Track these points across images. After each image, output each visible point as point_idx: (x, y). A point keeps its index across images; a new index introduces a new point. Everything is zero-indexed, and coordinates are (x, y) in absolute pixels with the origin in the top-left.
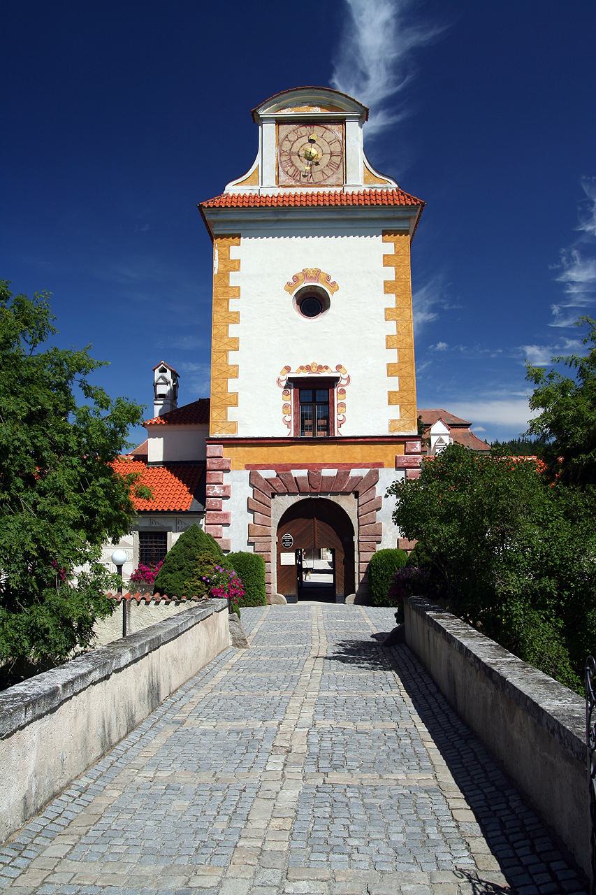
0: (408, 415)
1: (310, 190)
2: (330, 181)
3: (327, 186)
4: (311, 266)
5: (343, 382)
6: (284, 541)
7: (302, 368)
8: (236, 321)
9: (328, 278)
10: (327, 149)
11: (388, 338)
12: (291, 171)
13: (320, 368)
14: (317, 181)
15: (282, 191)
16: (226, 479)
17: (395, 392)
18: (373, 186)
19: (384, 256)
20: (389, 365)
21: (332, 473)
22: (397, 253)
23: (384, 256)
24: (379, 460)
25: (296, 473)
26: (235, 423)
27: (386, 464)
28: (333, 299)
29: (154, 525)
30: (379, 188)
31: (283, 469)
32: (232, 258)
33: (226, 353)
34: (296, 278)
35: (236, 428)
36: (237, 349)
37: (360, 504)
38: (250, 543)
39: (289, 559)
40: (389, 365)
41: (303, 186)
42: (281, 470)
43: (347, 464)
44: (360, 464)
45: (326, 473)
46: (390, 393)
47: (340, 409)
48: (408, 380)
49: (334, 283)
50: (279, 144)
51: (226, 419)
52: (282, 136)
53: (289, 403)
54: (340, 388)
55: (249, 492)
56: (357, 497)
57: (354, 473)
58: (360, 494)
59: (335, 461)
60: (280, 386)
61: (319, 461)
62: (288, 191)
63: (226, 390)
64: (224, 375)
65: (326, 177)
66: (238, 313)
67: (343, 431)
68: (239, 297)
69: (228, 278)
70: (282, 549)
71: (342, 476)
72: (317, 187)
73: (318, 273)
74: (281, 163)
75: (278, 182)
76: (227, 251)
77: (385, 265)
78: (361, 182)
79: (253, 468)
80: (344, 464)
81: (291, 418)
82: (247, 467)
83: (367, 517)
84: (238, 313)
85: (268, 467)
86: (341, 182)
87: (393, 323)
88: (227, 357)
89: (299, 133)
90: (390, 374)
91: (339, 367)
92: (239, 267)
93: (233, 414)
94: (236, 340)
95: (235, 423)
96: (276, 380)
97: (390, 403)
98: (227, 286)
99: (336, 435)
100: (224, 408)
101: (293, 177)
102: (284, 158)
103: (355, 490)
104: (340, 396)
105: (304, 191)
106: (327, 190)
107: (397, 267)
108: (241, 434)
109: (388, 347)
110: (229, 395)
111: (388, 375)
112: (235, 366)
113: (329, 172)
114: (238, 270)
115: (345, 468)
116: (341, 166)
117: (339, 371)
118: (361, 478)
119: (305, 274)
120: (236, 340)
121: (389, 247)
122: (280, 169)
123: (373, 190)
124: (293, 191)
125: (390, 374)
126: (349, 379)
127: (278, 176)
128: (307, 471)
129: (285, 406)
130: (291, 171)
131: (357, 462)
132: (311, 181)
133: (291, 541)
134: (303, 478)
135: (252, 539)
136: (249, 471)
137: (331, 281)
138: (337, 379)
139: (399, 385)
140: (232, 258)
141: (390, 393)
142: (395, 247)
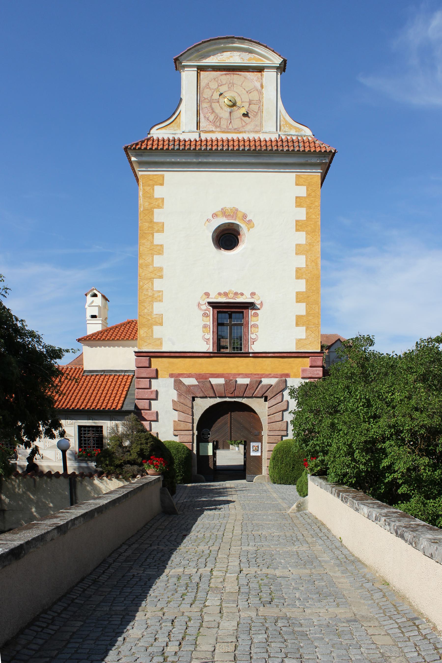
2: (248, 128)
3: (245, 132)
4: (229, 205)
7: (220, 294)
9: (245, 216)
10: (246, 98)
11: (298, 270)
12: (212, 118)
13: (236, 294)
14: (236, 127)
17: (302, 316)
18: (289, 133)
19: (297, 197)
21: (246, 381)
22: (309, 195)
23: (297, 197)
24: (286, 372)
25: (214, 381)
26: (160, 340)
30: (294, 135)
33: (151, 280)
34: (215, 215)
38: (176, 436)
41: (223, 132)
43: (258, 374)
44: (270, 374)
47: (253, 329)
49: (250, 221)
55: (174, 395)
56: (266, 400)
57: (265, 381)
58: (268, 398)
60: (201, 309)
61: (234, 371)
63: (152, 312)
65: (244, 124)
66: (162, 246)
68: (163, 231)
69: (153, 214)
76: (152, 191)
77: (296, 206)
80: (255, 374)
81: (210, 336)
82: (171, 376)
84: (162, 246)
85: (189, 376)
86: (258, 129)
88: (152, 284)
89: (219, 81)
92: (163, 204)
93: (157, 331)
94: (160, 269)
95: (160, 340)
97: (297, 325)
98: (151, 221)
99: (250, 351)
101: (214, 123)
105: (225, 136)
107: (309, 208)
110: (155, 316)
111: (297, 302)
116: (259, 114)
119: (224, 212)
120: (160, 269)
121: (302, 191)
127: (198, 123)
129: (205, 326)
131: (267, 373)
132: (230, 127)
134: (220, 385)
135: (176, 433)
137: (248, 219)
142: (307, 190)
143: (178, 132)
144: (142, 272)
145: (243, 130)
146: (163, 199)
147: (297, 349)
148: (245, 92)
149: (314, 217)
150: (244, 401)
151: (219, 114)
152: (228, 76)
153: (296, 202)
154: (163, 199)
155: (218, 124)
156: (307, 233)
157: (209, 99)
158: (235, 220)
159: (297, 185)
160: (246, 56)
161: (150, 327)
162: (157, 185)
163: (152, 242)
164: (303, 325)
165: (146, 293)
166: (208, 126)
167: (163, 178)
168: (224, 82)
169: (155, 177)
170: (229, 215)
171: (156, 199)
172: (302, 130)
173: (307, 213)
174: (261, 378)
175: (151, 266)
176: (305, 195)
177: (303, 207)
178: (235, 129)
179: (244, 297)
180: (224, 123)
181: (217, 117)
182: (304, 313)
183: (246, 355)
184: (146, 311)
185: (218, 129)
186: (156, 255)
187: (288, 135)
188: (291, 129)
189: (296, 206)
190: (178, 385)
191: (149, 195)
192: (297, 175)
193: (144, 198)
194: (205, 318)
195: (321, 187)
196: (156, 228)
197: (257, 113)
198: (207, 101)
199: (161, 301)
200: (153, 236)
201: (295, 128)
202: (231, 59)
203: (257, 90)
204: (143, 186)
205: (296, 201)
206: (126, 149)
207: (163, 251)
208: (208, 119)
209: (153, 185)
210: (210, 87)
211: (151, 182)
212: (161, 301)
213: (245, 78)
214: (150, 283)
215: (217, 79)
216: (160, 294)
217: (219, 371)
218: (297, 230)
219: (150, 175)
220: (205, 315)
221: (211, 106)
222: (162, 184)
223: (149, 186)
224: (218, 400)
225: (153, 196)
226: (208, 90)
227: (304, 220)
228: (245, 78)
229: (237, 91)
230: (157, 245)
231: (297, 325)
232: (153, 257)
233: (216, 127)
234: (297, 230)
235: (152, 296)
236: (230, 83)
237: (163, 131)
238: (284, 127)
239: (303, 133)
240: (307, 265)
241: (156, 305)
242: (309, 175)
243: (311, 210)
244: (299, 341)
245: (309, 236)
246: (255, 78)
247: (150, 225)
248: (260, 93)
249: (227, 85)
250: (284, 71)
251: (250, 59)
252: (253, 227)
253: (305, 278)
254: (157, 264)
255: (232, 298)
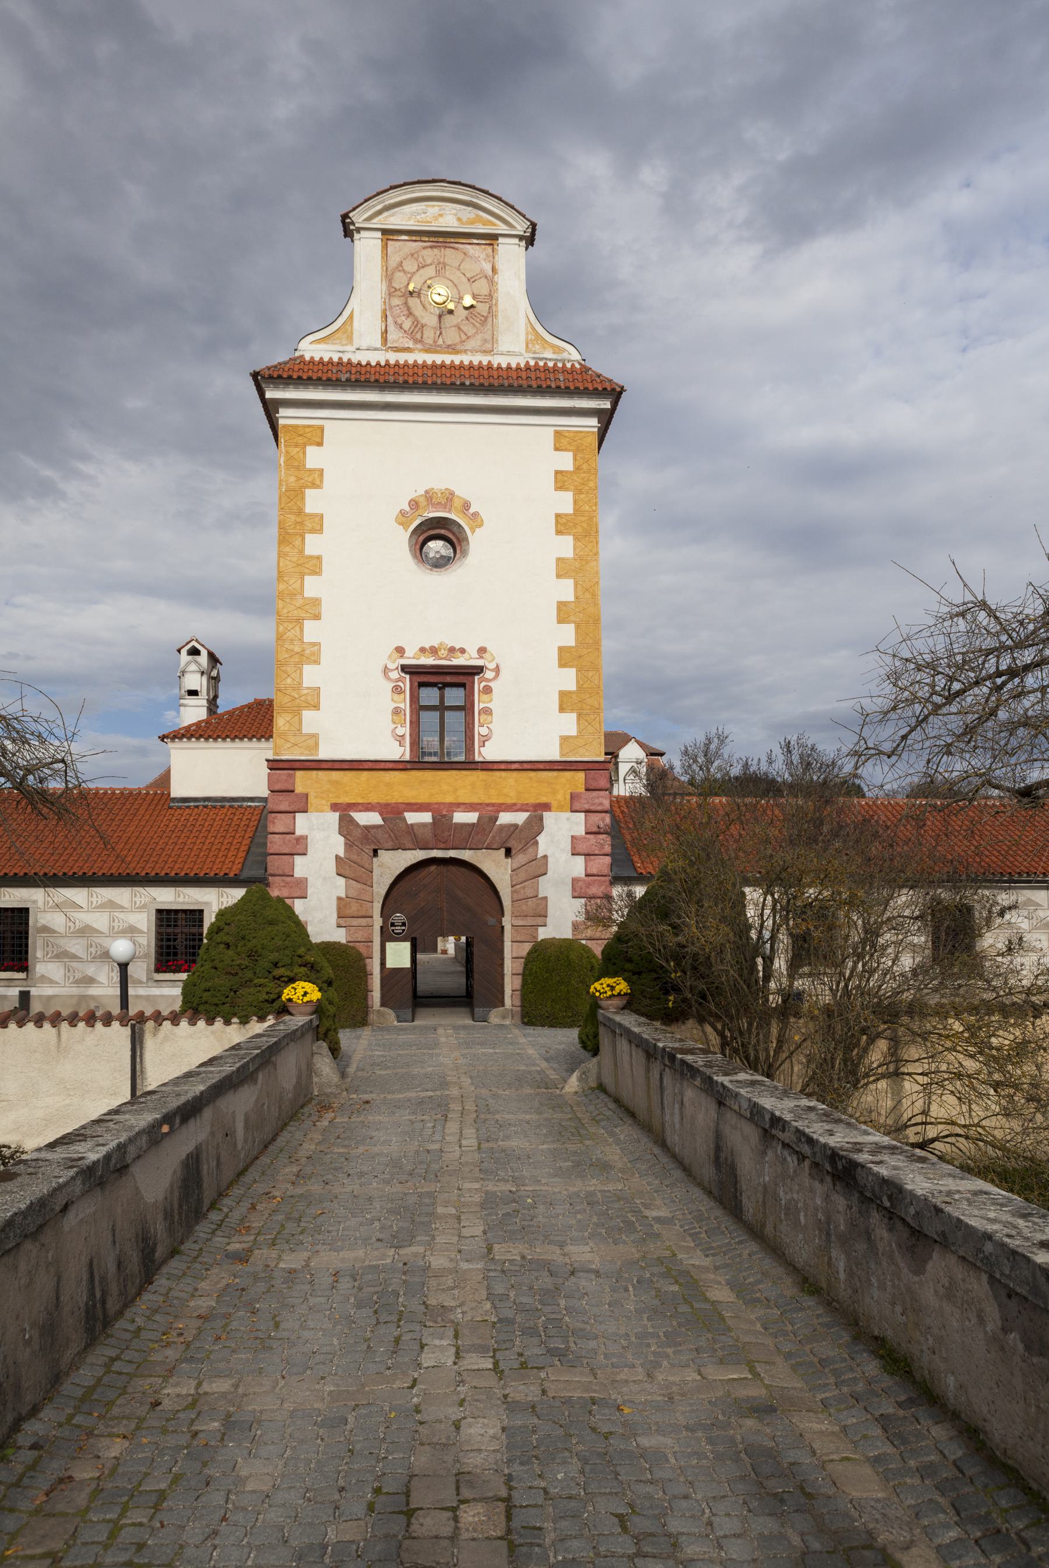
0: (590, 729)
1: (438, 359)
2: (471, 344)
3: (465, 351)
5: (489, 675)
6: (393, 925)
7: (423, 650)
8: (317, 571)
9: (466, 505)
11: (561, 605)
12: (407, 324)
13: (452, 650)
14: (449, 342)
15: (393, 358)
16: (302, 824)
17: (570, 692)
18: (541, 356)
19: (557, 472)
20: (561, 649)
21: (472, 817)
22: (578, 468)
23: (557, 472)
24: (544, 800)
25: (413, 818)
26: (315, 737)
27: (554, 804)
28: (476, 540)
29: (181, 899)
30: (550, 360)
31: (393, 812)
32: (309, 465)
34: (414, 504)
35: (317, 744)
36: (317, 617)
37: (515, 866)
39: (399, 955)
40: (561, 649)
42: (388, 813)
43: (493, 805)
44: (515, 804)
45: (461, 817)
46: (563, 694)
47: (483, 717)
48: (590, 674)
49: (476, 515)
50: (388, 276)
51: (300, 730)
52: (394, 261)
53: (402, 706)
54: (483, 684)
55: (338, 845)
56: (508, 853)
57: (505, 818)
58: (513, 852)
59: (475, 800)
60: (389, 679)
61: (449, 799)
62: (402, 358)
63: (300, 683)
64: (296, 659)
65: (464, 337)
66: (319, 558)
67: (488, 753)
68: (320, 531)
69: (303, 498)
70: (388, 935)
71: (489, 820)
72: (450, 353)
73: (450, 497)
74: (391, 308)
75: (385, 340)
76: (301, 455)
77: (557, 489)
78: (521, 347)
79: (344, 810)
80: (488, 805)
82: (335, 807)
83: (524, 888)
84: (319, 558)
85: (368, 807)
86: (488, 346)
87: (569, 584)
88: (302, 630)
89: (421, 259)
90: (562, 664)
91: (482, 651)
92: (322, 481)
94: (316, 602)
95: (315, 737)
96: (381, 668)
97: (562, 709)
98: (300, 512)
99: (477, 758)
100: (296, 712)
101: (411, 334)
102: (396, 301)
103: (508, 845)
104: (484, 697)
105: (430, 358)
106: (466, 359)
108: (325, 753)
109: (561, 620)
110: (305, 692)
112: (314, 644)
113: (469, 330)
114: (319, 487)
115: (490, 812)
116: (490, 319)
117: (482, 657)
118: (516, 826)
119: (429, 496)
120: (316, 602)
122: (390, 319)
123: (541, 364)
124: (410, 358)
125: (562, 664)
126: (497, 670)
127: (385, 333)
128: (430, 814)
129: (396, 711)
130: (407, 324)
131: (509, 801)
132: (440, 342)
133: (404, 924)
134: (424, 825)
136: (337, 814)
137: (472, 511)
138: (479, 670)
139: (578, 682)
140: (309, 465)
141: (563, 694)
142: (575, 459)
143: (348, 348)
144: (283, 608)
145: (462, 348)
146: (321, 471)
147: (562, 755)
148: (465, 280)
149: (587, 508)
150: (466, 855)
151: (420, 319)
152: (436, 251)
153: (556, 482)
154: (321, 471)
155: (418, 336)
156: (576, 539)
157: (403, 290)
158: (450, 512)
159: (556, 449)
160: (469, 213)
161: (297, 712)
162: (311, 444)
163: (301, 551)
164: (572, 711)
165: (291, 647)
166: (401, 340)
167: (322, 431)
168: (429, 261)
169: (307, 430)
170: (439, 503)
171: (310, 470)
172: (564, 350)
173: (575, 502)
174: (498, 812)
175: (299, 597)
176: (570, 467)
177: (567, 490)
178: (449, 346)
179: (466, 655)
180: (429, 336)
181: (416, 323)
182: (572, 687)
183: (470, 765)
184: (289, 681)
185: (419, 346)
186: (310, 574)
187: (541, 359)
188: (545, 348)
189: (557, 489)
190: (347, 825)
191: (296, 464)
192: (556, 432)
193: (288, 469)
194: (396, 696)
195: (599, 449)
196: (308, 524)
197: (486, 318)
198: (399, 293)
199: (317, 662)
200: (303, 539)
201: (553, 346)
202: (441, 220)
203: (486, 277)
204: (286, 446)
205: (556, 478)
206: (255, 375)
207: (320, 568)
208: (401, 328)
209: (304, 446)
210: (405, 268)
211: (300, 440)
212: (317, 662)
213: (465, 254)
214: (297, 629)
215: (416, 256)
216: (316, 648)
217: (423, 798)
218: (559, 532)
219: (298, 426)
220: (397, 690)
221: (406, 303)
222: (320, 444)
223: (296, 446)
224: (420, 855)
225: (304, 465)
226: (401, 274)
227: (570, 515)
228: (465, 254)
229: (451, 277)
230: (311, 557)
231: (562, 709)
232: (302, 579)
233: (416, 341)
234: (559, 532)
235: (301, 654)
236: (439, 263)
237: (322, 346)
238: (534, 345)
239: (565, 356)
240: (576, 597)
241: (307, 669)
242: (577, 432)
243: (582, 496)
244: (564, 740)
245: (579, 544)
246: (483, 256)
247: (299, 520)
248: (491, 282)
249: (433, 267)
250: (532, 245)
251: (472, 222)
252: (481, 525)
253: (574, 622)
254: (309, 592)
255: (445, 659)
